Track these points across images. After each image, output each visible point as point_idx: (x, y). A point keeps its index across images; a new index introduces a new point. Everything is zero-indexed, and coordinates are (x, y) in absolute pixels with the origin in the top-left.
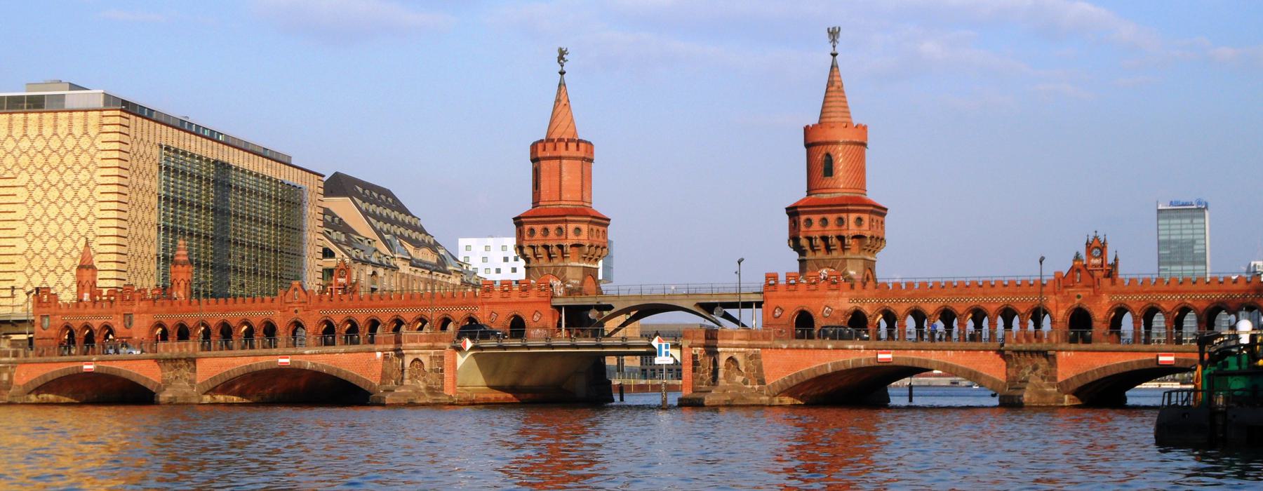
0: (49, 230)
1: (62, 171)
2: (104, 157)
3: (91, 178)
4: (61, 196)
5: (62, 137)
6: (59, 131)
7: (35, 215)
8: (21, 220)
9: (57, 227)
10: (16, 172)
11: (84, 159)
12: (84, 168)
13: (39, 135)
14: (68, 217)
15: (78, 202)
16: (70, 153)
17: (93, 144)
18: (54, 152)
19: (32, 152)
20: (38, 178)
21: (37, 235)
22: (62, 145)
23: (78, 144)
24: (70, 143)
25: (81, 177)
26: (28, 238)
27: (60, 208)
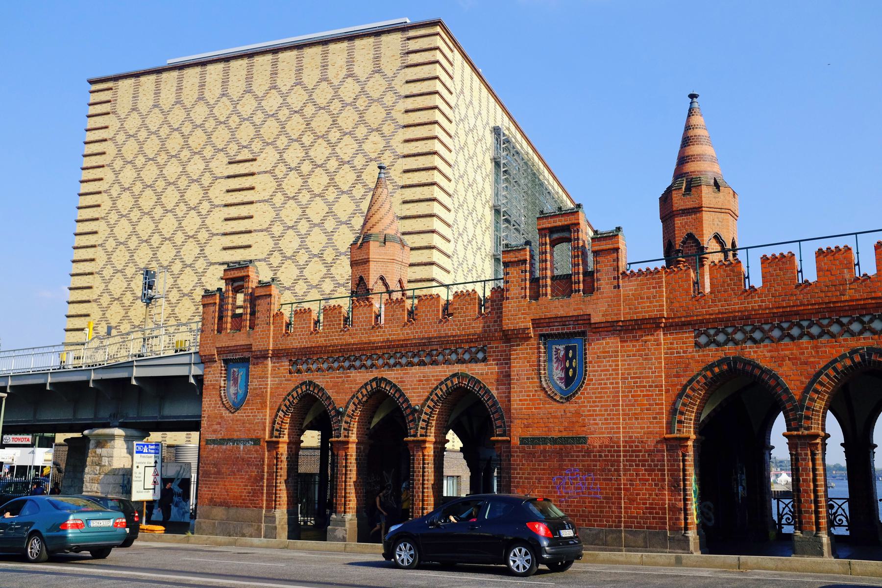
0: (310, 245)
1: (333, 140)
2: (410, 107)
3: (387, 147)
4: (332, 182)
5: (336, 82)
6: (331, 73)
7: (286, 220)
8: (262, 231)
9: (323, 239)
10: (256, 150)
11: (375, 115)
12: (373, 130)
13: (296, 84)
14: (344, 219)
15: (362, 191)
16: (349, 107)
17: (390, 88)
18: (321, 108)
19: (284, 114)
20: (294, 155)
21: (288, 254)
22: (336, 95)
23: (363, 90)
24: (350, 89)
25: (367, 147)
26: (272, 260)
27: (330, 205)
